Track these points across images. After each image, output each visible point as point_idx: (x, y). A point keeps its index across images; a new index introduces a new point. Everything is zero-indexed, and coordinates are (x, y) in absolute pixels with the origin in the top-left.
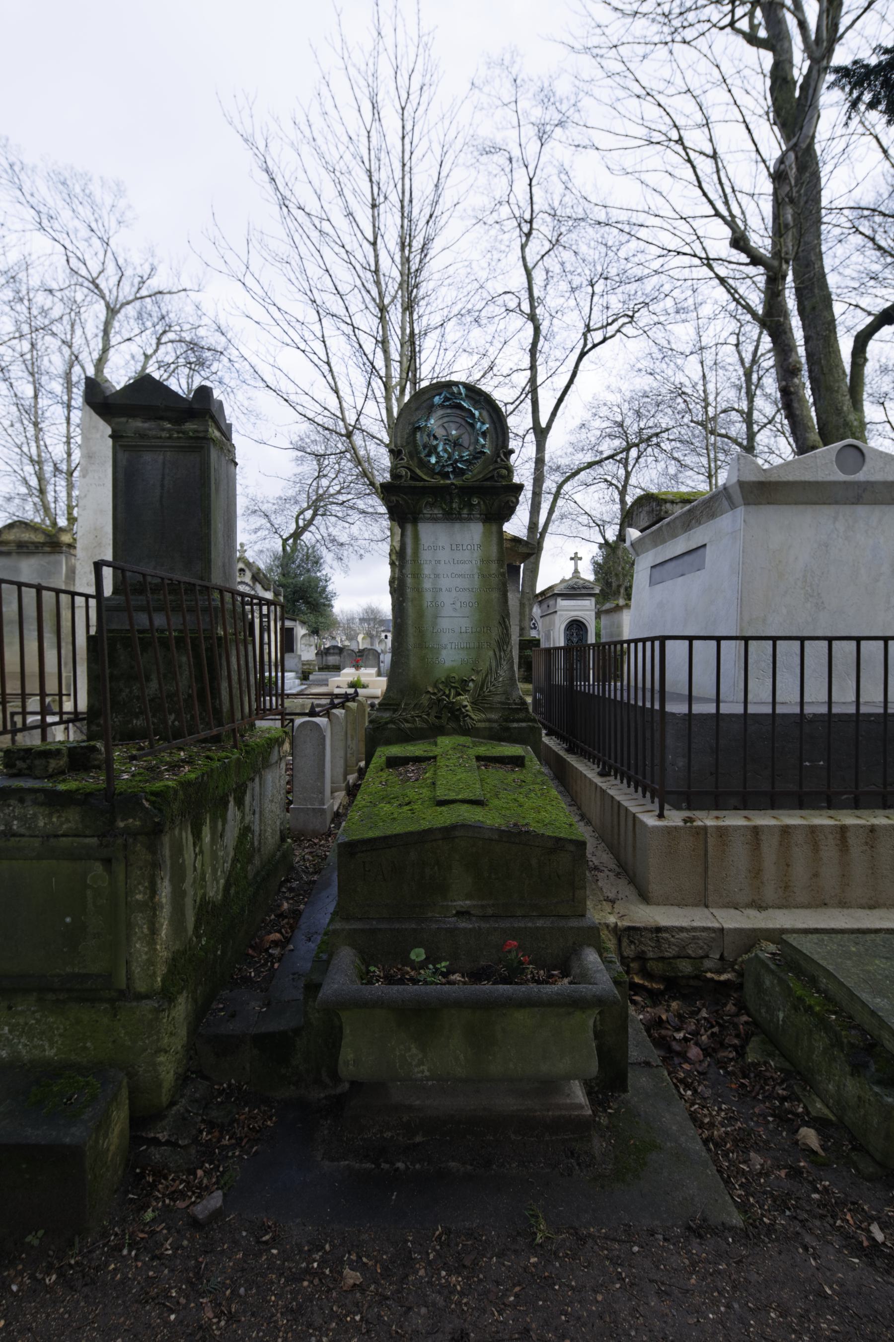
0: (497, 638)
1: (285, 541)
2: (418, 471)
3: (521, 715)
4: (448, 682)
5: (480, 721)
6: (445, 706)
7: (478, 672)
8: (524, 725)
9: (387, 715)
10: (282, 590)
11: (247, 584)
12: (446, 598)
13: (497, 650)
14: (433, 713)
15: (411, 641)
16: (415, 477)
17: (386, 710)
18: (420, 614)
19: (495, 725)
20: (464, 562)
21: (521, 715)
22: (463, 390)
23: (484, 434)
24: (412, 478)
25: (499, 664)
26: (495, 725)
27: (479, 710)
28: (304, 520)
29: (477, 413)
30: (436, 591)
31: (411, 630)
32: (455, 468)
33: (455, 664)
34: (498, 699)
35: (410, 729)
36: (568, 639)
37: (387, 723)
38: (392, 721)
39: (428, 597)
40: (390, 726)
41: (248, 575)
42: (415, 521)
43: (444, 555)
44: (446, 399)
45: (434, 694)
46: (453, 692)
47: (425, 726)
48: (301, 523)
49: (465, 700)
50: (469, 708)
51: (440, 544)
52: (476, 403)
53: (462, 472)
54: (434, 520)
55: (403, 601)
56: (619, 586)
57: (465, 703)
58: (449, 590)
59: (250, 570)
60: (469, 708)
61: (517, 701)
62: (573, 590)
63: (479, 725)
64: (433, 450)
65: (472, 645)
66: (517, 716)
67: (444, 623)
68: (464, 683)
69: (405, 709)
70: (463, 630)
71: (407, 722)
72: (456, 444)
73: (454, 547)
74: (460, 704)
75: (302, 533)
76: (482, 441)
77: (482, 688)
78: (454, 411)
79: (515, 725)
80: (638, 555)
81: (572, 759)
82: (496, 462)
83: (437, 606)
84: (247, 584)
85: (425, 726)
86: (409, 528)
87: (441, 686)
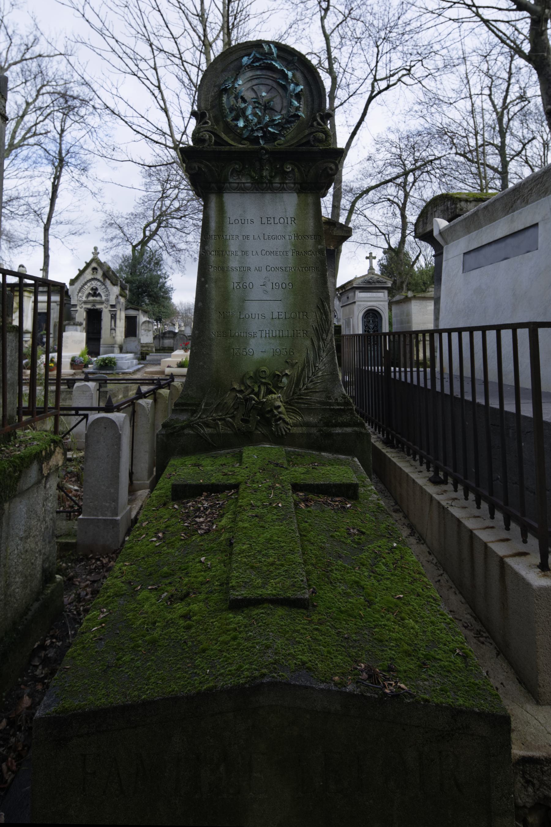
0: (315, 325)
1: (134, 247)
2: (223, 136)
3: (346, 418)
4: (257, 377)
5: (295, 425)
6: (253, 407)
7: (293, 366)
8: (349, 430)
9: (183, 417)
10: (128, 286)
11: (98, 280)
12: (255, 279)
13: (315, 340)
15: (214, 328)
17: (182, 411)
18: (225, 297)
19: (314, 430)
20: (276, 238)
21: (346, 418)
22: (274, 50)
23: (298, 96)
24: (216, 143)
25: (317, 356)
26: (314, 430)
27: (294, 412)
28: (150, 231)
29: (290, 74)
30: (244, 270)
31: (214, 316)
32: (266, 133)
33: (265, 355)
34: (316, 397)
35: (211, 435)
37: (183, 428)
38: (190, 426)
39: (234, 277)
40: (186, 431)
41: (100, 273)
42: (220, 192)
43: (252, 230)
44: (256, 59)
45: (241, 392)
46: (263, 389)
47: (229, 431)
48: (148, 233)
49: (277, 399)
51: (249, 217)
52: (289, 64)
53: (273, 137)
54: (242, 190)
55: (206, 282)
56: (402, 283)
57: (278, 403)
58: (259, 269)
59: (101, 268)
60: (282, 409)
61: (340, 400)
62: (368, 284)
63: (295, 430)
64: (241, 114)
66: (340, 419)
67: (253, 308)
68: (276, 378)
69: (205, 411)
70: (276, 315)
71: (208, 426)
73: (265, 220)
75: (148, 241)
76: (296, 103)
77: (297, 384)
78: (264, 72)
79: (338, 430)
82: (312, 126)
83: (244, 287)
84: (98, 280)
85: (229, 431)
86: (213, 199)
87: (248, 382)
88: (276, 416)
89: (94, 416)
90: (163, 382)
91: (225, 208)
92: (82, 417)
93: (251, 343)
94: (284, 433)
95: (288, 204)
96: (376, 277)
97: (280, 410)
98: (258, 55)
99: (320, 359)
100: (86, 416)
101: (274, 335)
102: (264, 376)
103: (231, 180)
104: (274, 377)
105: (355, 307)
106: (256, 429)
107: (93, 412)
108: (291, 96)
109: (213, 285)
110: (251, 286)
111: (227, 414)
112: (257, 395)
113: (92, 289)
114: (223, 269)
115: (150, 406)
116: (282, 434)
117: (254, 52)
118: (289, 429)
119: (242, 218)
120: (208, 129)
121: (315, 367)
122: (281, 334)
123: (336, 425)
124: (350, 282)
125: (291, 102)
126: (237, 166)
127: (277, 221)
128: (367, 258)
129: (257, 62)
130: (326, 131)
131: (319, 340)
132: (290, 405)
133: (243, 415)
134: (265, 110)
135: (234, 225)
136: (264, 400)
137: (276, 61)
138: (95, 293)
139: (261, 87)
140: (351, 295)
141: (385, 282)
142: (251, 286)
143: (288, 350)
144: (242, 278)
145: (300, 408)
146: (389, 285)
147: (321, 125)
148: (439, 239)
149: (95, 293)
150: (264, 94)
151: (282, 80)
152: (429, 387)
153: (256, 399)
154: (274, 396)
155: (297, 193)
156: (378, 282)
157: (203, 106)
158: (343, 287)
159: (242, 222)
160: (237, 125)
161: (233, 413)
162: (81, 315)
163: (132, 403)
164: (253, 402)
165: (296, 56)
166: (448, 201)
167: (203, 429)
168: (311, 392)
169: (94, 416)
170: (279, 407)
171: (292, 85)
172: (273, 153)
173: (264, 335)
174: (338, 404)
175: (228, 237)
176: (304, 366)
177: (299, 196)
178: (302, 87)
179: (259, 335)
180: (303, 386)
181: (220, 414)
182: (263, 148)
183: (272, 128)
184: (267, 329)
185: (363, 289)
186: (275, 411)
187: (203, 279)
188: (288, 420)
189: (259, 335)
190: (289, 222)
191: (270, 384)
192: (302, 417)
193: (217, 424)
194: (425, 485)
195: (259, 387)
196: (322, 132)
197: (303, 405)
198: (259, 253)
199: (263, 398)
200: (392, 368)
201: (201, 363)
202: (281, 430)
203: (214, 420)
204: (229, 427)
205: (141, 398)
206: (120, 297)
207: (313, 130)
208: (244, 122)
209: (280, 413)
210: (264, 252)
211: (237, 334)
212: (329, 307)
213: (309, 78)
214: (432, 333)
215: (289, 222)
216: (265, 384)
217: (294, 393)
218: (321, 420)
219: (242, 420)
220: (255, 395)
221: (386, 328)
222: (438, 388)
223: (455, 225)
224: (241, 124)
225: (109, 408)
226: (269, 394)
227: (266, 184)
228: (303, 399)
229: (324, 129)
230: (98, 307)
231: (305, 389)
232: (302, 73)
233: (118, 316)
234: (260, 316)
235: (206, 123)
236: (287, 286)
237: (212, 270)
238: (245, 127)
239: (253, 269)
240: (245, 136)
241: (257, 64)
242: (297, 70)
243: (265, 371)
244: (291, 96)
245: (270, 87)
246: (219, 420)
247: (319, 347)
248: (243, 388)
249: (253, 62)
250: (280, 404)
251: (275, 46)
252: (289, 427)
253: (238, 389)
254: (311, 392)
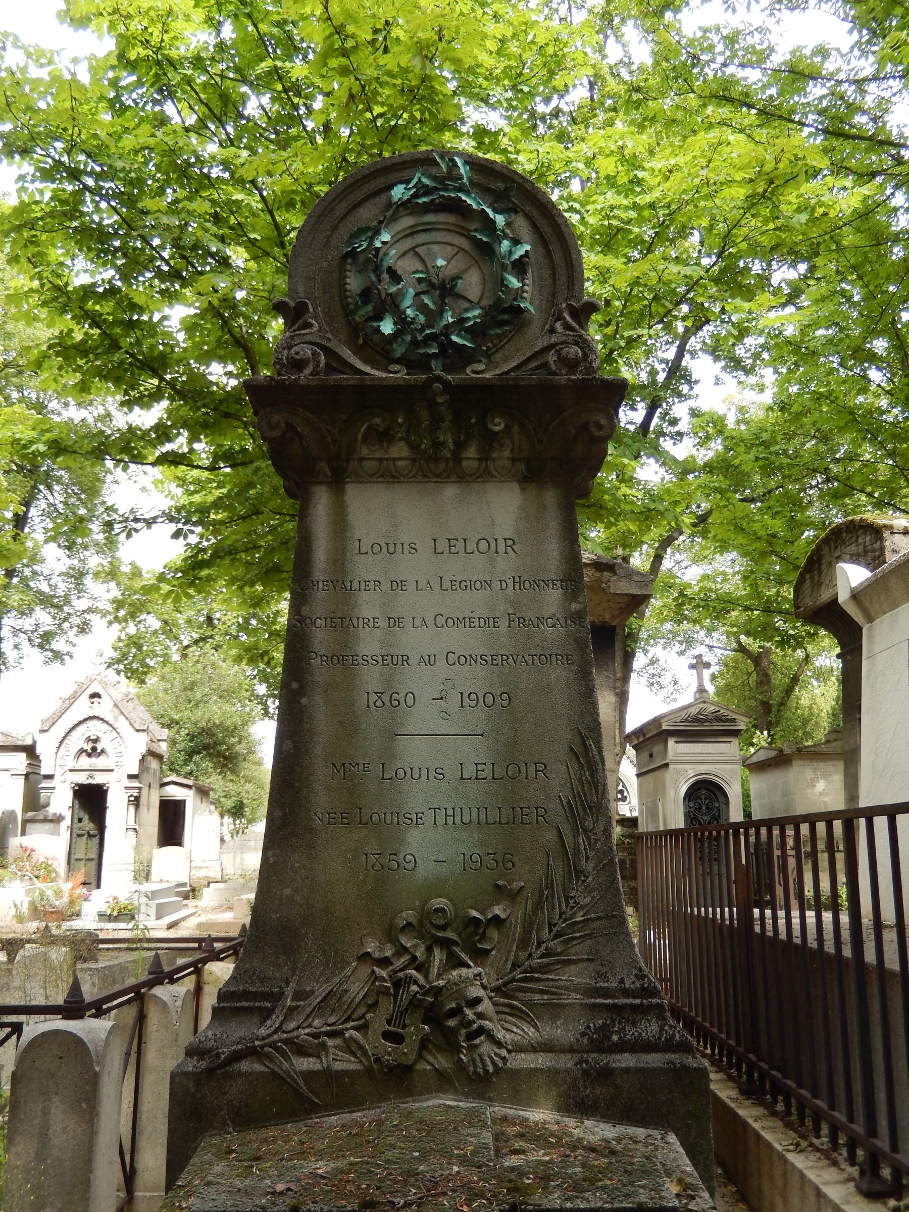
0: (565, 794)
2: (347, 353)
5: (519, 1049)
6: (414, 1003)
8: (654, 1060)
9: (240, 1031)
12: (420, 683)
13: (566, 830)
14: (379, 1021)
16: (336, 364)
17: (238, 1011)
18: (349, 727)
20: (469, 585)
22: (463, 170)
23: (520, 267)
24: (329, 369)
27: (516, 1012)
29: (500, 220)
30: (394, 661)
32: (447, 346)
33: (444, 870)
35: (308, 1075)
36: (690, 817)
37: (237, 1057)
39: (371, 679)
40: (245, 1066)
42: (337, 482)
43: (414, 567)
44: (421, 190)
45: (384, 962)
50: (486, 1006)
51: (406, 540)
52: (501, 201)
53: (464, 357)
54: (389, 476)
55: (301, 692)
57: (476, 991)
58: (429, 661)
60: (486, 1006)
65: (494, 815)
66: (631, 1033)
67: (414, 753)
71: (301, 1051)
72: (445, 290)
73: (442, 545)
74: (459, 994)
76: (514, 282)
78: (442, 217)
79: (626, 1060)
80: (870, 619)
81: (748, 1113)
82: (552, 331)
83: (393, 701)
86: (322, 502)
88: (470, 1023)
89: (34, 1027)
90: (218, 946)
91: (350, 518)
92: (9, 1029)
93: (410, 840)
94: (491, 1069)
95: (502, 508)
96: (712, 708)
97: (480, 1008)
98: (425, 181)
99: (578, 878)
100: (17, 1029)
101: (466, 819)
102: (441, 922)
103: (365, 452)
104: (466, 926)
105: (668, 775)
106: (420, 1057)
107: (36, 1018)
108: (504, 267)
109: (319, 699)
110: (410, 701)
111: (347, 1020)
112: (422, 968)
113: (89, 739)
114: (345, 660)
115: (179, 1003)
116: (486, 1071)
117: (418, 175)
118: (503, 1059)
119: (391, 541)
120: (309, 338)
121: (567, 898)
122: (483, 817)
123: (624, 1047)
124: (656, 721)
125: (503, 279)
126: (378, 421)
127: (471, 546)
128: (692, 667)
129: (424, 195)
130: (585, 341)
132: (506, 995)
133: (389, 1022)
134: (442, 297)
135: (370, 556)
136: (441, 983)
137: (468, 193)
138: (94, 749)
139: (435, 248)
140: (657, 749)
141: (734, 720)
142: (410, 701)
143: (499, 857)
144: (389, 682)
145: (530, 1004)
147: (572, 329)
148: (853, 611)
149: (94, 749)
150: (440, 262)
151: (481, 232)
152: (847, 952)
153: (420, 978)
154: (464, 971)
155: (520, 482)
156: (719, 719)
157: (301, 288)
158: (640, 732)
159: (391, 548)
160: (378, 329)
161: (363, 1017)
162: (61, 801)
163: (139, 996)
164: (414, 988)
165: (514, 181)
166: (865, 533)
167: (288, 1059)
168: (558, 962)
169: (34, 1027)
170: (478, 1001)
171: (505, 244)
172: (458, 392)
173: (441, 820)
174: (626, 993)
175: (356, 586)
176: (541, 897)
177: (523, 490)
178: (528, 248)
179: (428, 818)
180: (539, 945)
181: (332, 1020)
182: (439, 379)
183: (459, 335)
184: (449, 806)
185: (685, 736)
186: (467, 1011)
187: (295, 685)
188: (500, 1034)
189: (428, 818)
190: (501, 548)
191: (456, 943)
192: (535, 1026)
193: (324, 1046)
194: (848, 1202)
195: (429, 950)
196: (576, 344)
197: (537, 997)
198: (430, 622)
199: (439, 976)
200: (756, 911)
201: (287, 891)
202: (482, 1060)
203: (316, 1036)
204: (353, 1054)
205: (161, 983)
206: (150, 758)
207: (554, 339)
208: (395, 324)
209: (480, 1016)
210: (441, 620)
211: (375, 818)
212: (600, 751)
213: (547, 230)
214: (849, 818)
215: (501, 548)
216: (446, 944)
217: (515, 966)
218: (583, 1034)
219: (387, 1036)
220: (418, 969)
221: (736, 815)
222: (870, 956)
223: (885, 576)
224: (387, 327)
225: (73, 1008)
226: (455, 967)
227: (447, 461)
228: (538, 980)
229: (581, 336)
230: (99, 779)
231: (543, 956)
232: (528, 217)
233: (143, 801)
234: (432, 774)
235: (309, 325)
236: (498, 698)
237: (316, 662)
238: (396, 335)
239: (414, 660)
240: (398, 355)
241: (425, 199)
242: (516, 212)
243: (442, 910)
244: (504, 267)
245: (456, 250)
246: (331, 1035)
247: (576, 847)
248: (389, 953)
249: (416, 196)
250: (481, 993)
251: (466, 163)
252: (504, 1053)
253: (376, 955)
254: (558, 962)
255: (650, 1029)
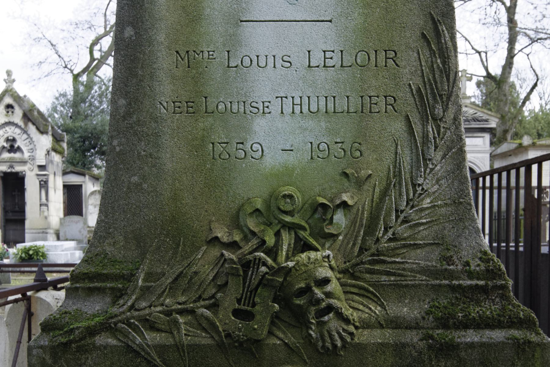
4: (273, 211)
5: (366, 325)
6: (263, 282)
7: (360, 183)
8: (498, 335)
14: (229, 301)
15: (165, 90)
17: (91, 291)
19: (412, 337)
26: (412, 337)
27: (364, 293)
33: (291, 159)
34: (416, 259)
35: (161, 349)
40: (101, 340)
46: (287, 239)
47: (204, 339)
49: (322, 262)
50: (334, 286)
57: (324, 272)
60: (334, 286)
61: (475, 265)
63: (364, 336)
65: (342, 104)
66: (475, 311)
67: (260, 40)
68: (321, 211)
69: (146, 291)
70: (317, 59)
71: (153, 327)
74: (309, 275)
77: (371, 229)
79: (471, 336)
85: (204, 339)
87: (252, 224)
88: (318, 301)
93: (256, 128)
94: (339, 343)
97: (328, 288)
99: (426, 166)
101: (314, 108)
102: (289, 208)
106: (270, 333)
116: (335, 346)
118: (351, 334)
121: (414, 186)
123: (465, 325)
131: (424, 120)
132: (353, 276)
133: (239, 301)
136: (291, 264)
143: (347, 146)
146: (493, 125)
153: (270, 261)
154: (313, 255)
161: (213, 296)
164: (263, 269)
168: (404, 246)
170: (326, 281)
173: (288, 109)
174: (471, 275)
176: (389, 185)
181: (182, 299)
184: (297, 95)
188: (348, 312)
189: (275, 107)
191: (304, 229)
192: (382, 306)
193: (176, 322)
195: (278, 234)
197: (384, 278)
199: (287, 259)
201: (135, 179)
202: (331, 336)
203: (168, 313)
204: (204, 330)
209: (329, 295)
211: (221, 107)
216: (292, 227)
217: (362, 250)
218: (428, 313)
219: (236, 313)
226: (303, 252)
228: (384, 262)
231: (390, 240)
234: (279, 62)
243: (291, 197)
246: (181, 312)
247: (425, 136)
248: (237, 238)
250: (329, 274)
252: (351, 328)
253: (225, 239)
254: (404, 246)
255: (489, 308)
